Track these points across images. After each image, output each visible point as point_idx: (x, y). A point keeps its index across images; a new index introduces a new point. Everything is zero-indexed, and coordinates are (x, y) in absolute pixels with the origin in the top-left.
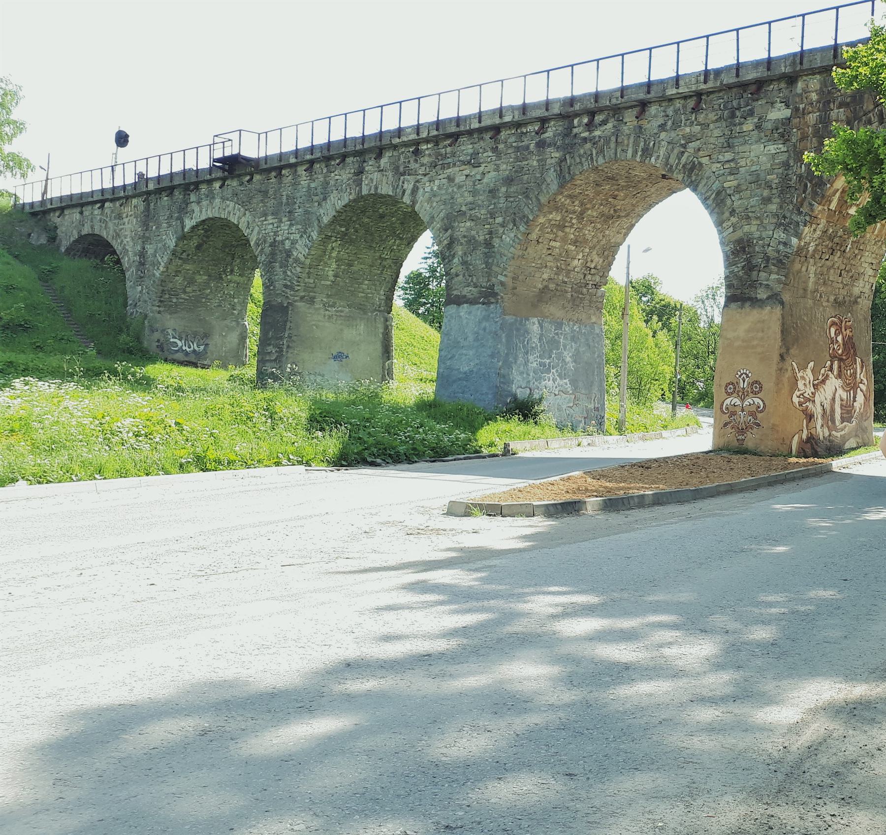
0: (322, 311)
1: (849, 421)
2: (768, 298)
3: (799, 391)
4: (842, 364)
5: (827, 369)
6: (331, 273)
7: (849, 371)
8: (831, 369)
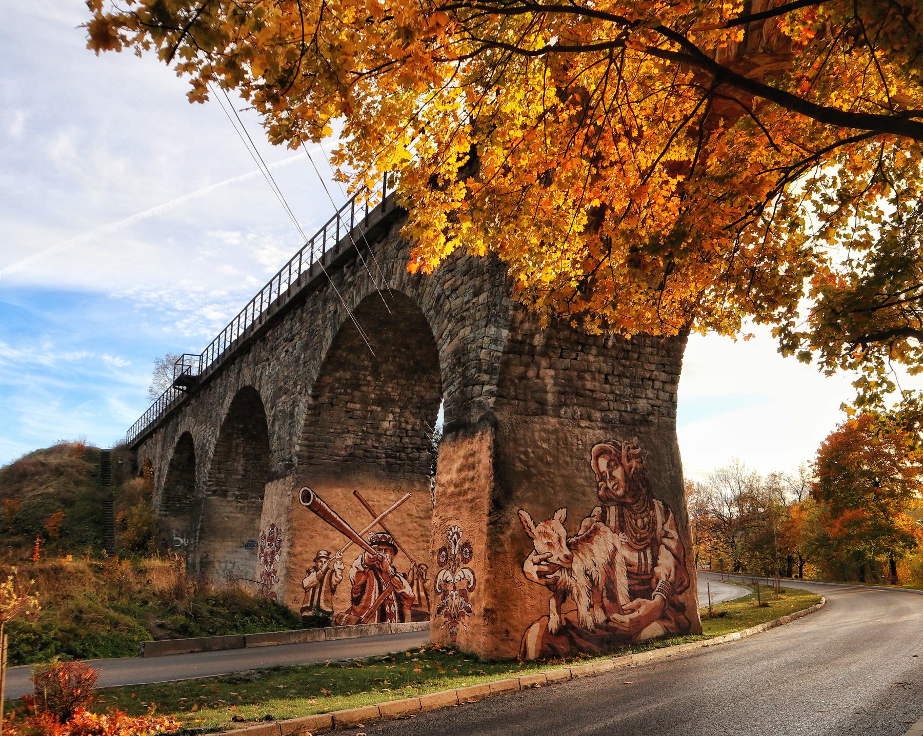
0: (234, 504)
1: (647, 594)
2: (481, 420)
3: (537, 554)
4: (625, 511)
5: (594, 519)
6: (240, 468)
7: (639, 521)
8: (603, 519)
